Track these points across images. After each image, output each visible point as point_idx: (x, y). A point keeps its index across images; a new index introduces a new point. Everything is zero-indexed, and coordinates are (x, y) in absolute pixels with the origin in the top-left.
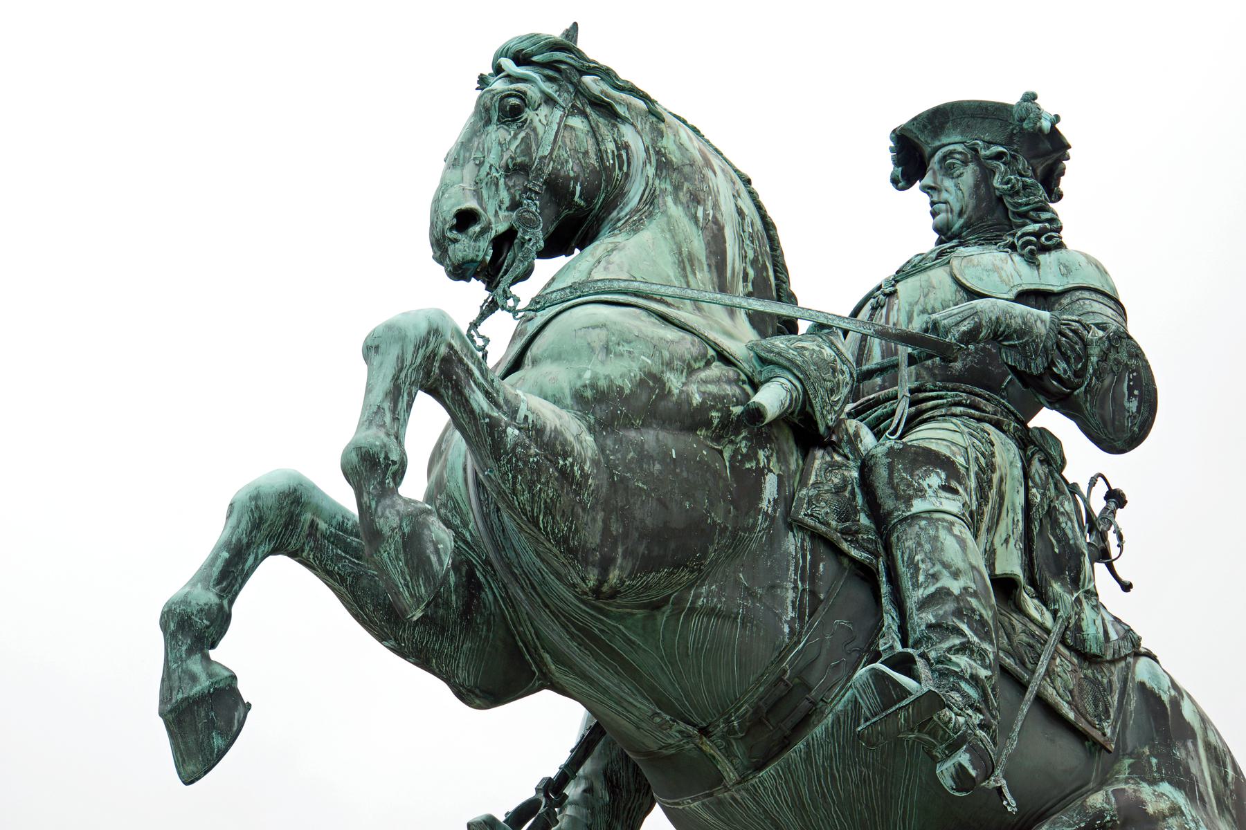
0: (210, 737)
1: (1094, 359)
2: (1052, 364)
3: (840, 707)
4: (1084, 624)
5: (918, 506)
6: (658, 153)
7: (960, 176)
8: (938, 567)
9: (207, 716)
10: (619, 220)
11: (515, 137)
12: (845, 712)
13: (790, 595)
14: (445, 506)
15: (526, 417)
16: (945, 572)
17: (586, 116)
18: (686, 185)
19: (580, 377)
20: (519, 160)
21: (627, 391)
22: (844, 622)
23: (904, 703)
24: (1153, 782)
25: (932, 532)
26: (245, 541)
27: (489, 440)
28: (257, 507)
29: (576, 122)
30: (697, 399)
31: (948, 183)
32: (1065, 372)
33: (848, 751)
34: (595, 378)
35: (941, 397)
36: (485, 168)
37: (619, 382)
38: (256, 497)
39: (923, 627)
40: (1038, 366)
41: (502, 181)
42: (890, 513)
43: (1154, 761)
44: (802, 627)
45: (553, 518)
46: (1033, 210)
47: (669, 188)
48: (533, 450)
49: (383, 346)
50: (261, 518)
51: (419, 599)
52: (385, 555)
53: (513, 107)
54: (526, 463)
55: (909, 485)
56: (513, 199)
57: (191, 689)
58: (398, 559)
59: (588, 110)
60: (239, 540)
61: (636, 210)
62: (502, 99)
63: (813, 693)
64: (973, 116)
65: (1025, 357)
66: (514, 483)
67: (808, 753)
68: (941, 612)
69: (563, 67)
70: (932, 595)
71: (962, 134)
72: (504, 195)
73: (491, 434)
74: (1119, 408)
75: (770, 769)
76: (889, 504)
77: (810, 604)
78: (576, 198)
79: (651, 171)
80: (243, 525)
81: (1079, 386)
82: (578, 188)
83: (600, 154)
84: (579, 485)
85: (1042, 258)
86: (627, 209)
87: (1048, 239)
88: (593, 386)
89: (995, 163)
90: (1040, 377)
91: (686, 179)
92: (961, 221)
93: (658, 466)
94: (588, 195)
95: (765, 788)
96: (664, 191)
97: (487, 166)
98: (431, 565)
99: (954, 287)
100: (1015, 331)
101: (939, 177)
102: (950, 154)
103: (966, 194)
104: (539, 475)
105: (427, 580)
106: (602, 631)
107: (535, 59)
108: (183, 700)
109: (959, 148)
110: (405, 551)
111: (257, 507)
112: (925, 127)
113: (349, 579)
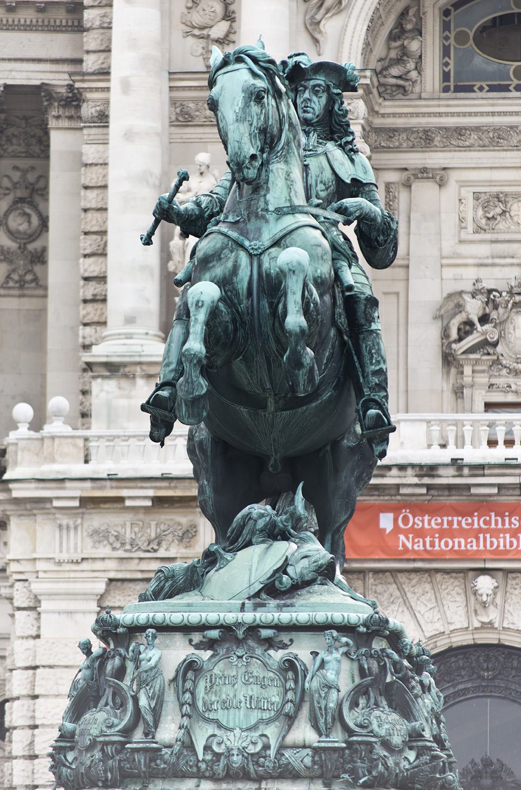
2: (379, 236)
5: (374, 327)
7: (321, 97)
8: (380, 358)
10: (278, 152)
13: (327, 354)
14: (231, 292)
19: (316, 271)
31: (315, 99)
34: (321, 271)
42: (362, 326)
49: (296, 272)
51: (305, 391)
61: (283, 148)
64: (331, 70)
65: (370, 229)
71: (326, 76)
72: (259, 143)
74: (388, 255)
75: (288, 412)
76: (363, 321)
88: (321, 277)
89: (337, 97)
97: (253, 126)
102: (319, 85)
105: (312, 386)
106: (273, 360)
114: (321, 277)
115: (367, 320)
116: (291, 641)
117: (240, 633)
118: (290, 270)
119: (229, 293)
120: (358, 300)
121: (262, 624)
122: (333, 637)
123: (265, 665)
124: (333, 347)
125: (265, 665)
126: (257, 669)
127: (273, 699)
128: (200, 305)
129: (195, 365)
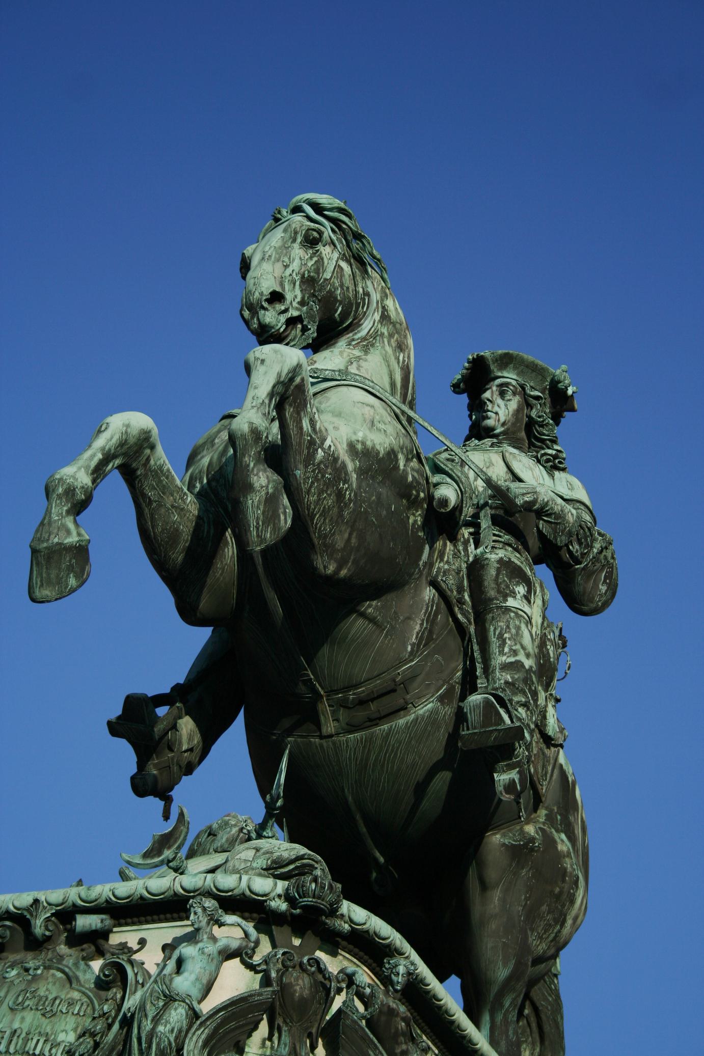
0: (68, 576)
1: (595, 550)
3: (421, 712)
4: (548, 714)
5: (511, 602)
6: (383, 307)
8: (518, 647)
9: (70, 561)
10: (353, 340)
11: (311, 258)
12: (423, 716)
13: (418, 628)
15: (330, 446)
16: (522, 652)
17: (351, 265)
18: (396, 336)
19: (355, 433)
20: (312, 274)
21: (381, 455)
22: (440, 658)
23: (499, 727)
24: (558, 831)
25: (517, 623)
26: (113, 451)
27: (306, 452)
28: (126, 432)
29: (343, 264)
30: (410, 479)
31: (499, 401)
32: (577, 551)
33: (413, 742)
34: (365, 437)
35: (500, 536)
36: (288, 271)
37: (378, 447)
38: (128, 426)
39: (502, 681)
40: (561, 540)
41: (298, 283)
42: (492, 600)
43: (559, 817)
44: (417, 651)
45: (325, 520)
46: (549, 440)
47: (386, 333)
48: (329, 470)
49: (267, 362)
50: (126, 440)
52: (250, 502)
53: (314, 238)
54: (323, 476)
55: (508, 587)
56: (303, 298)
57: (66, 538)
58: (258, 508)
59: (352, 261)
60: (110, 449)
61: (364, 339)
62: (308, 229)
63: (408, 697)
64: (527, 366)
65: (555, 531)
66: (311, 487)
67: (388, 734)
68: (516, 677)
69: (344, 226)
70: (511, 663)
71: (518, 375)
72: (298, 292)
73: (308, 448)
76: (492, 593)
77: (427, 638)
78: (336, 315)
79: (377, 316)
80: (114, 441)
81: (580, 563)
82: (340, 309)
83: (356, 292)
84: (345, 504)
85: (557, 473)
86: (359, 335)
87: (560, 463)
89: (534, 402)
90: (560, 548)
91: (397, 333)
92: (502, 429)
93: (385, 512)
94: (345, 315)
95: (347, 746)
96: (382, 335)
98: (279, 520)
99: (505, 469)
100: (555, 513)
101: (495, 396)
102: (507, 385)
103: (511, 413)
104: (327, 488)
105: (274, 529)
107: (326, 213)
108: (58, 544)
109: (514, 383)
110: (265, 504)
111: (126, 432)
112: (497, 360)
113: (155, 504)
114: (363, 443)
115: (499, 592)
116: (142, 942)
117: (38, 927)
118: (256, 359)
119: (214, 484)
120: (486, 562)
121: (80, 903)
122: (204, 909)
123: (70, 979)
124: (431, 620)
125: (70, 979)
126: (50, 987)
127: (61, 1037)
128: (103, 429)
129: (59, 497)
